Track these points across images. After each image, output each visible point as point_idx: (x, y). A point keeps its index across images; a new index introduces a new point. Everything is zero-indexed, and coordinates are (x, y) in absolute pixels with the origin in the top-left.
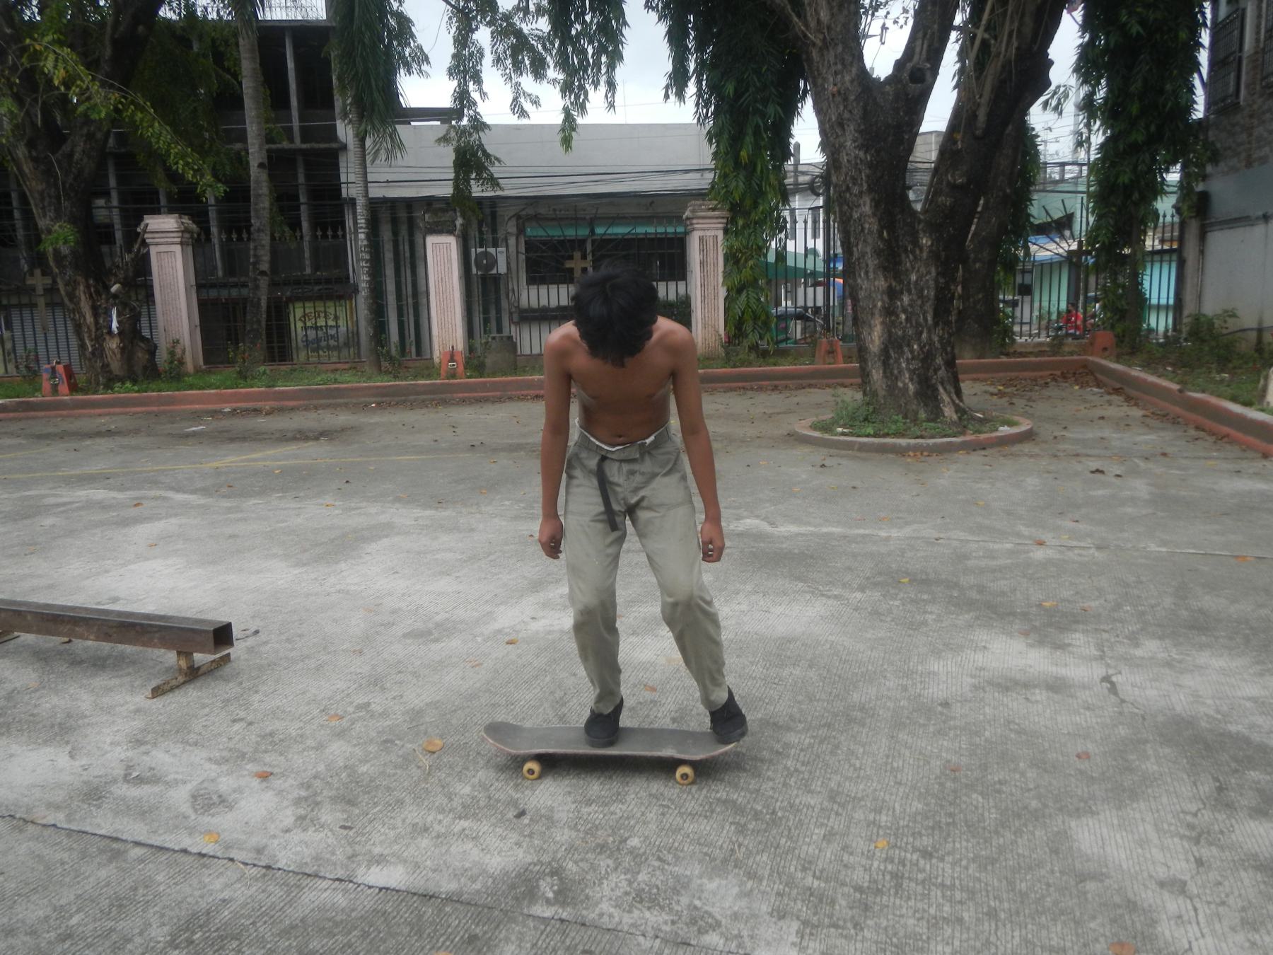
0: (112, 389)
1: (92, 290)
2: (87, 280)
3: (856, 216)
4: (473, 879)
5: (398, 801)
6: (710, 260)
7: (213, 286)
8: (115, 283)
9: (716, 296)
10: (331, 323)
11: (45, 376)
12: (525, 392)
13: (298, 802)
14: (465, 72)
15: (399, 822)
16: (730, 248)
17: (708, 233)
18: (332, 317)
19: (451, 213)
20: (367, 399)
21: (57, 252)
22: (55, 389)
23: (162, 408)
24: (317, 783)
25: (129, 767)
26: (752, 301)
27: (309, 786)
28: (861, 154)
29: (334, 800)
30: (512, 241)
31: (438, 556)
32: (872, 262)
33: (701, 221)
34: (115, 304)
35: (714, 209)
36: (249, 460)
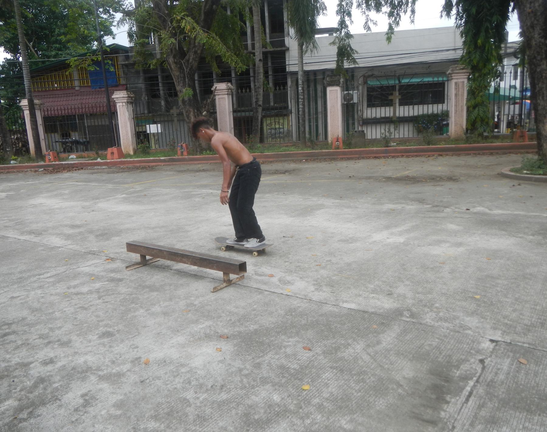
2: (194, 111)
4: (380, 309)
5: (348, 287)
7: (239, 111)
10: (281, 127)
11: (179, 148)
12: (368, 155)
13: (314, 285)
14: (344, 12)
15: (350, 293)
19: (338, 76)
20: (302, 158)
22: (182, 154)
24: (319, 280)
25: (255, 272)
27: (317, 281)
29: (326, 285)
30: (360, 88)
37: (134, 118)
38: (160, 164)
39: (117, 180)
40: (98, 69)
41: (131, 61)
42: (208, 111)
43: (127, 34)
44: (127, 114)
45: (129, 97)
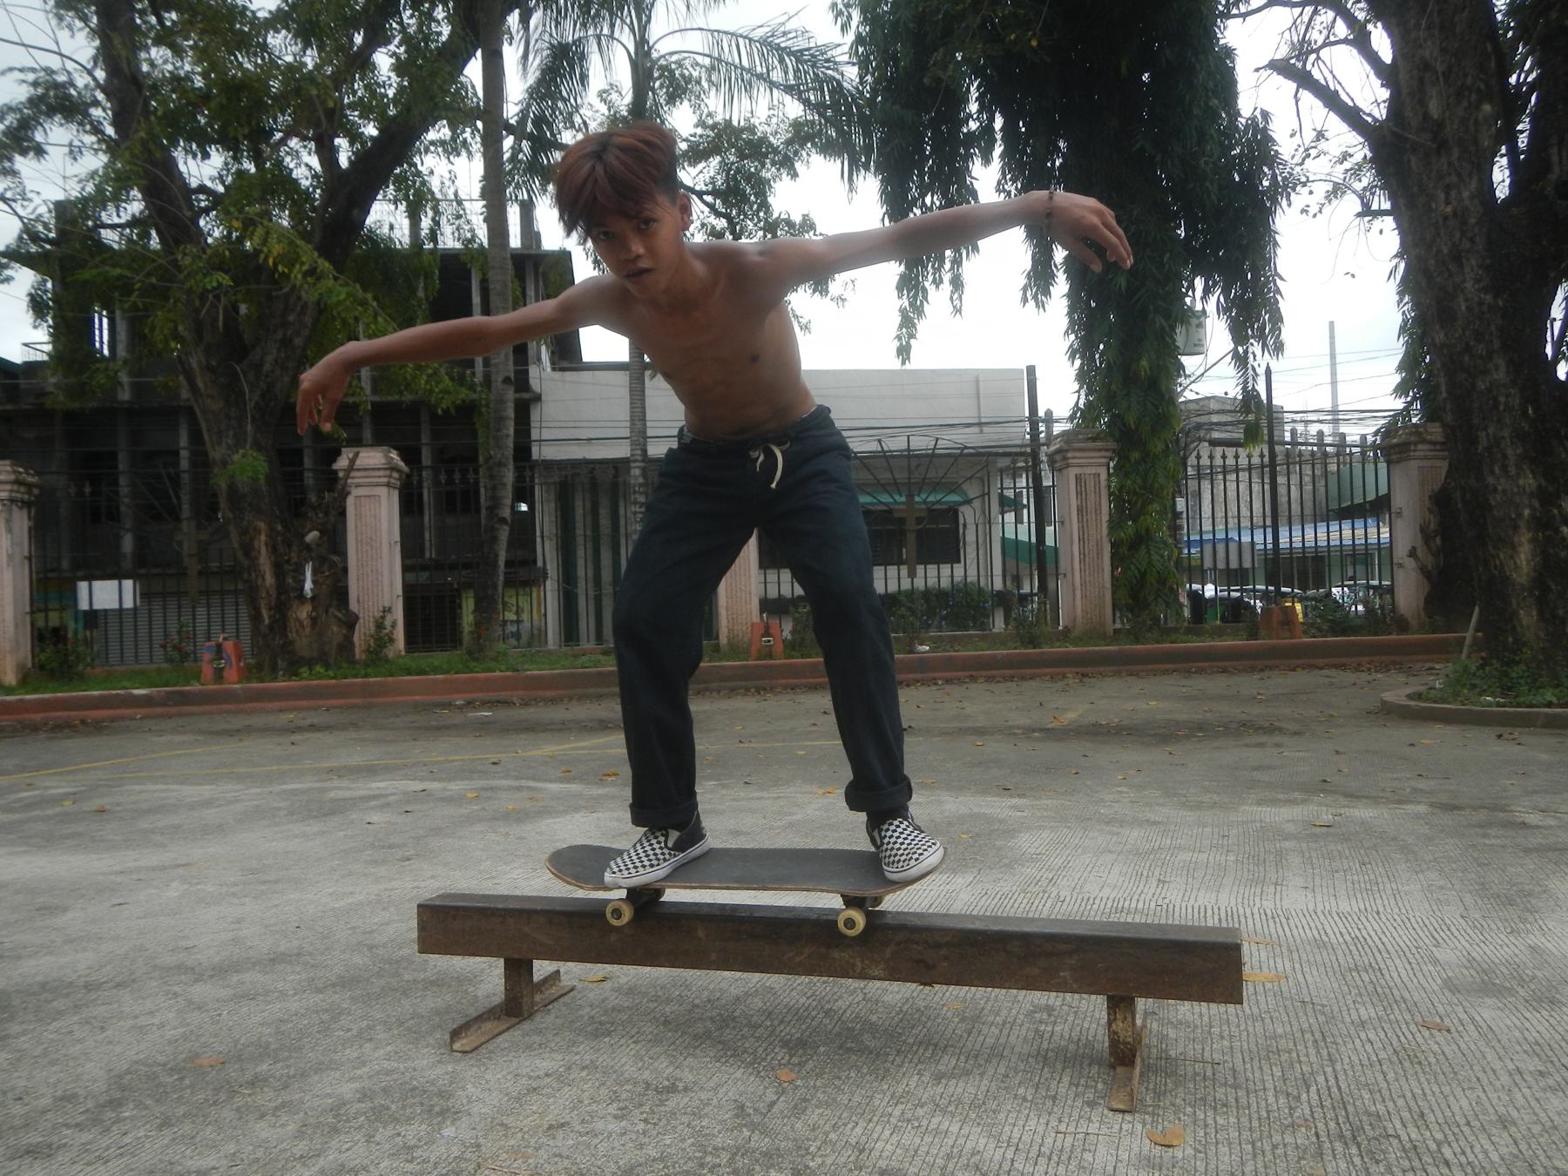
0: (297, 675)
2: (272, 529)
3: (1481, 386)
6: (1091, 506)
8: (310, 531)
9: (1100, 554)
11: (207, 656)
16: (1120, 490)
17: (1088, 471)
18: (514, 609)
21: (232, 488)
23: (369, 700)
26: (1155, 557)
28: (1488, 298)
31: (1186, 856)
32: (1512, 452)
33: (1078, 454)
35: (1094, 439)
36: (583, 748)
37: (30, 558)
43: (27, 299)
44: (5, 541)
45: (18, 482)
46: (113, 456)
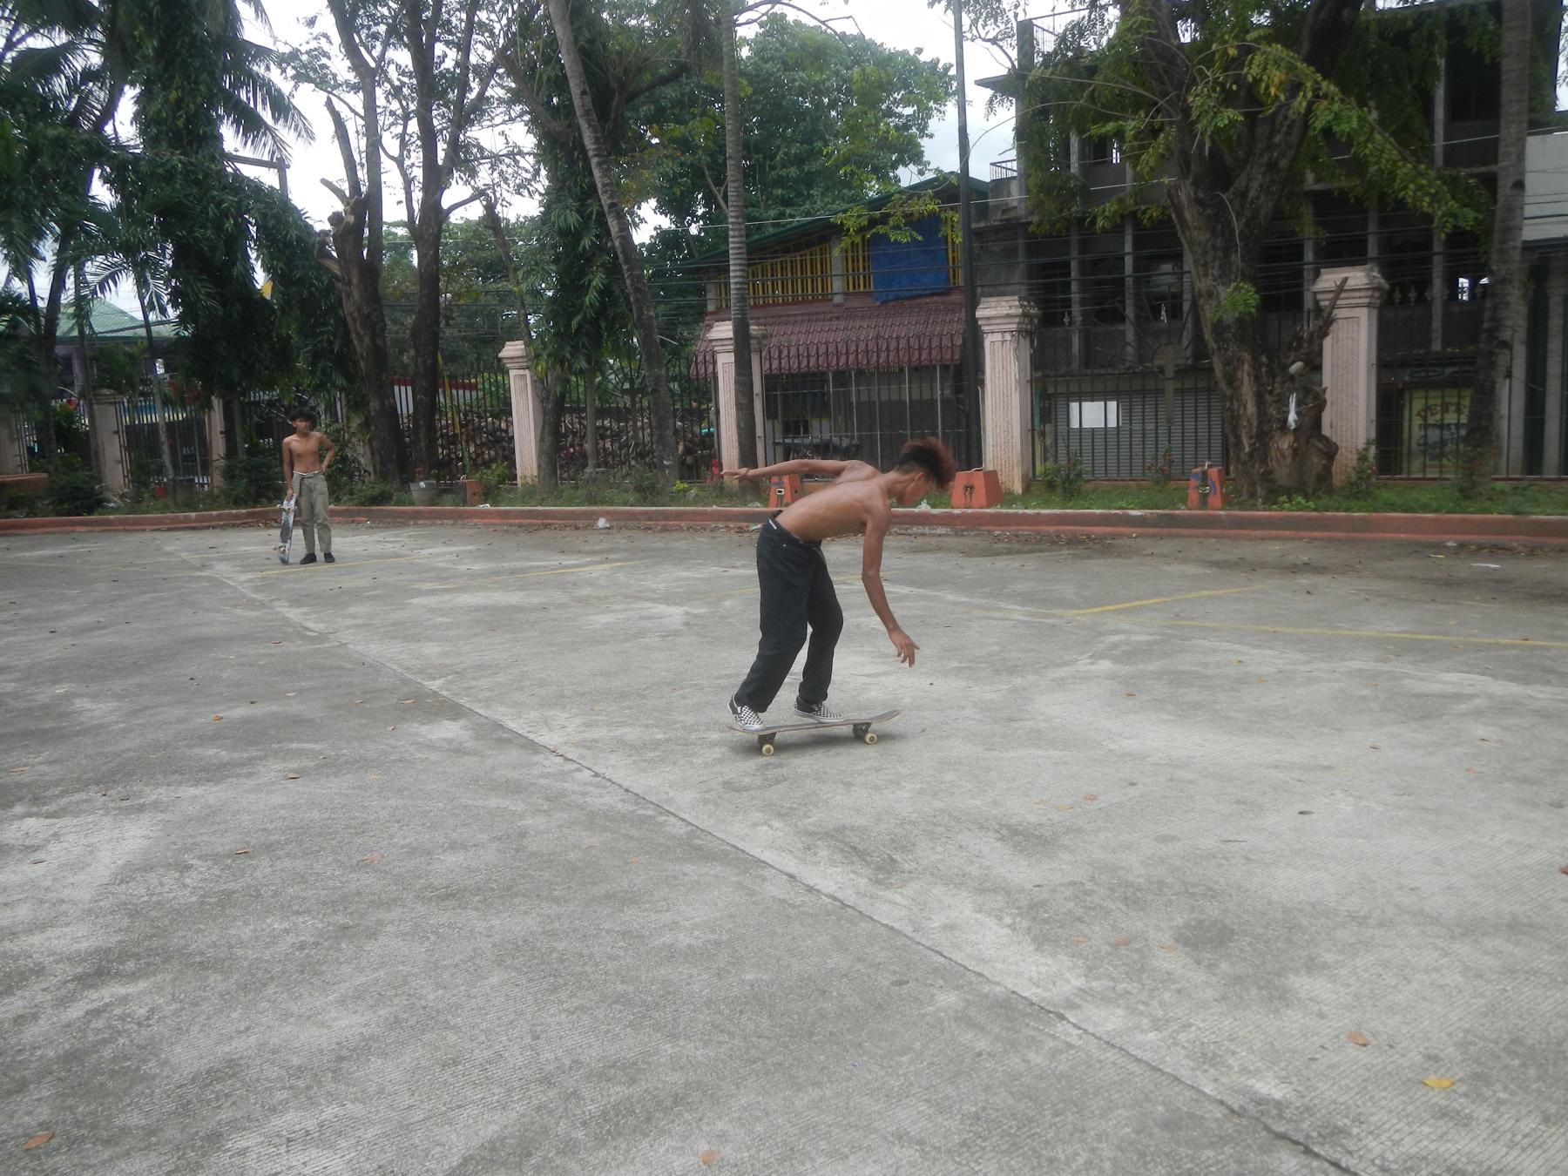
0: (1275, 503)
1: (1264, 369)
2: (1255, 359)
7: (1404, 364)
8: (1293, 362)
11: (1194, 482)
22: (1204, 501)
34: (1296, 390)
37: (1031, 381)
38: (1126, 530)
39: (1021, 587)
40: (920, 238)
41: (995, 219)
42: (1307, 362)
44: (1014, 368)
45: (1024, 315)
46: (1067, 265)
